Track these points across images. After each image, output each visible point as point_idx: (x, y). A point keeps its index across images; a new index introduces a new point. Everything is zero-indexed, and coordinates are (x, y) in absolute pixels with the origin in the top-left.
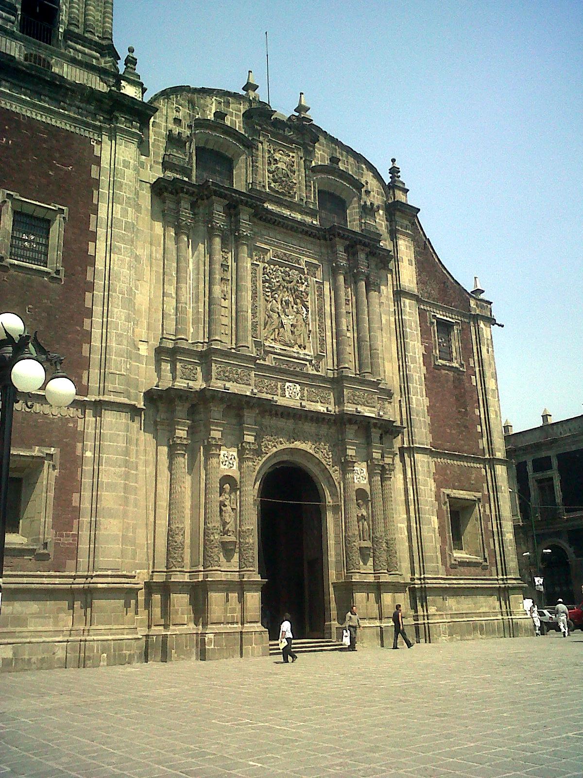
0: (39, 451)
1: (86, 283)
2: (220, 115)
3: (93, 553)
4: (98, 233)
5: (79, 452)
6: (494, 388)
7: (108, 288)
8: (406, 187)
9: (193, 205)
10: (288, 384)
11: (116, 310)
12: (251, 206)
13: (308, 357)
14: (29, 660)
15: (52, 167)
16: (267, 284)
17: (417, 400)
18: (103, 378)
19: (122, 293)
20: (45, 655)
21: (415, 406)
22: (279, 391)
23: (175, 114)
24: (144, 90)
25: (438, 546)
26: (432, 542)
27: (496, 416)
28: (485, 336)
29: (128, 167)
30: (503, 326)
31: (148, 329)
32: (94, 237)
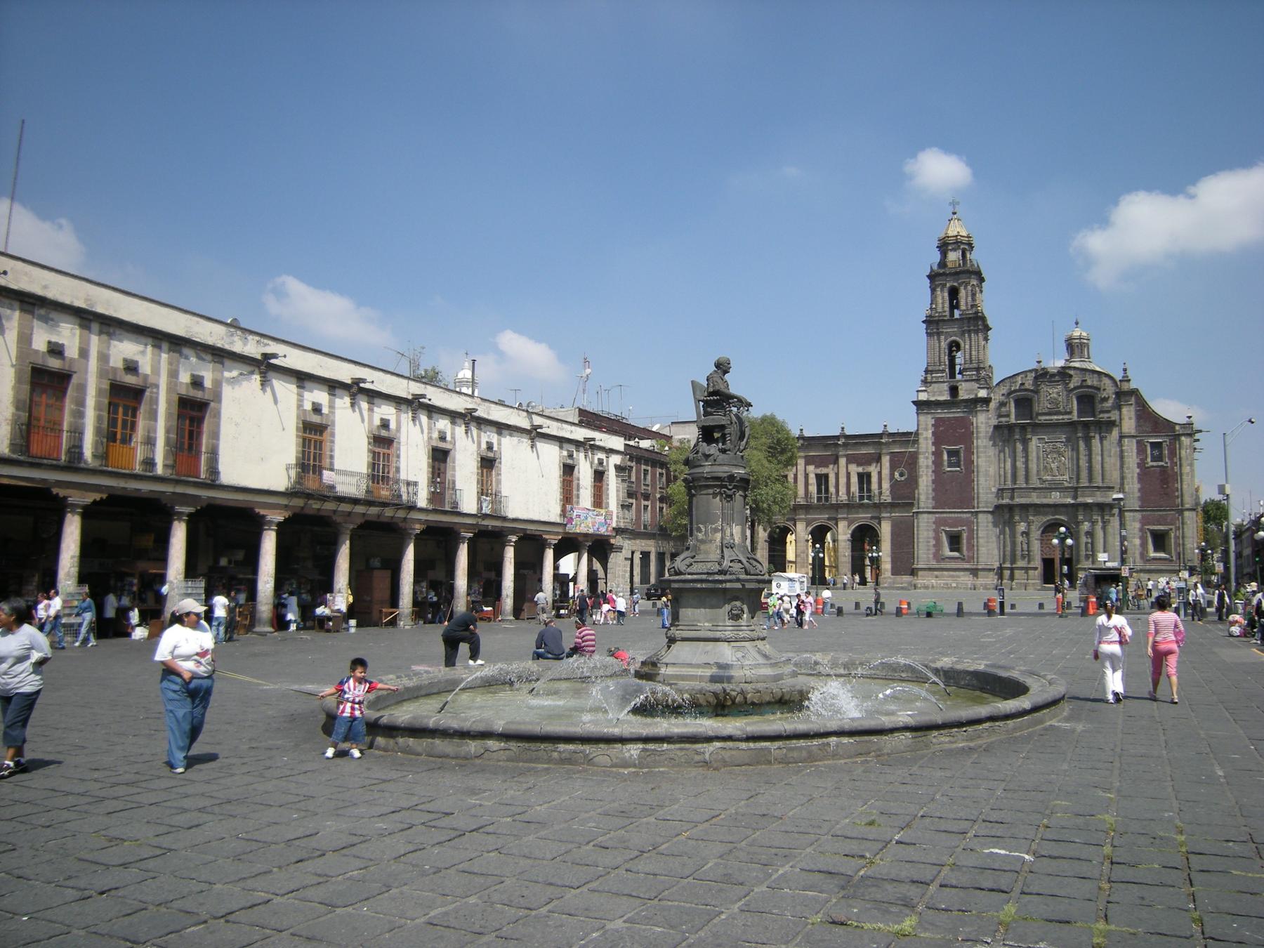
2: (1022, 384)
9: (1009, 430)
27: (1189, 485)
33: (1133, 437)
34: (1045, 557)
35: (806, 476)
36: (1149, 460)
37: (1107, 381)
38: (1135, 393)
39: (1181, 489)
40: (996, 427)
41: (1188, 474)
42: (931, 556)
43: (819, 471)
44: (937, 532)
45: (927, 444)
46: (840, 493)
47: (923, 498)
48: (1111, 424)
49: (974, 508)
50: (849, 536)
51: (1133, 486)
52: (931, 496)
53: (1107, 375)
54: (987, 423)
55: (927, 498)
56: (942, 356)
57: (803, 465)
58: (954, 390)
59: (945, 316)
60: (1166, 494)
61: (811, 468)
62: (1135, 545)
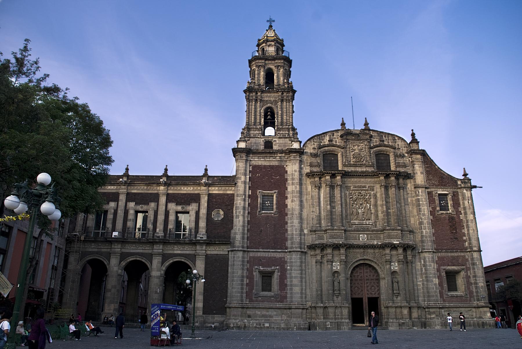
0: (274, 268)
1: (285, 213)
3: (292, 297)
4: (288, 196)
5: (286, 268)
6: (473, 219)
7: (292, 214)
8: (418, 141)
10: (361, 235)
11: (294, 221)
12: (340, 174)
13: (370, 224)
14: (274, 327)
15: (272, 179)
16: (351, 199)
17: (426, 231)
18: (292, 243)
19: (296, 215)
20: (278, 326)
21: (424, 234)
22: (358, 239)
23: (313, 146)
24: (300, 142)
25: (438, 291)
26: (434, 289)
27: (474, 231)
28: (467, 196)
29: (296, 172)
30: (482, 187)
31: (307, 224)
32: (287, 198)
33: (426, 188)
34: (354, 296)
35: (126, 212)
36: (438, 208)
37: (399, 142)
38: (423, 153)
39: (469, 234)
40: (308, 175)
41: (472, 220)
42: (244, 295)
43: (139, 208)
44: (250, 271)
45: (245, 187)
46: (158, 230)
47: (238, 237)
48: (408, 176)
49: (287, 248)
50: (163, 272)
51: (427, 231)
52: (246, 236)
53: (400, 138)
54: (300, 172)
55: (243, 238)
56: (258, 118)
57: (124, 201)
58: (268, 144)
59: (264, 88)
60: (456, 238)
61: (132, 205)
62: (435, 284)
